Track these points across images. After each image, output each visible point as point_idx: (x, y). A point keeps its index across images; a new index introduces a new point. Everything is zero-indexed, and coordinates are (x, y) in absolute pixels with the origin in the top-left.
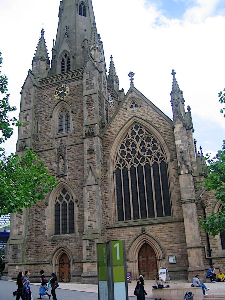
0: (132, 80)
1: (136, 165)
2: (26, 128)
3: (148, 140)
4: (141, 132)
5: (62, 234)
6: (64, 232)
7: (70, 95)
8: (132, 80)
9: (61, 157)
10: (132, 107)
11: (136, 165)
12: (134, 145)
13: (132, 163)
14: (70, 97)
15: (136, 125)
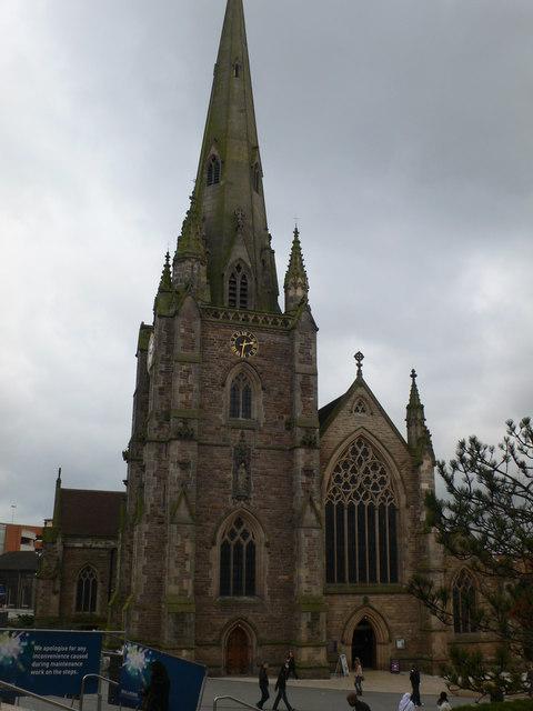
0: (359, 365)
1: (356, 503)
2: (187, 397)
3: (375, 467)
4: (365, 453)
5: (235, 594)
6: (238, 592)
7: (260, 355)
8: (359, 365)
10: (357, 410)
11: (356, 503)
12: (354, 471)
13: (350, 498)
14: (259, 360)
15: (361, 440)
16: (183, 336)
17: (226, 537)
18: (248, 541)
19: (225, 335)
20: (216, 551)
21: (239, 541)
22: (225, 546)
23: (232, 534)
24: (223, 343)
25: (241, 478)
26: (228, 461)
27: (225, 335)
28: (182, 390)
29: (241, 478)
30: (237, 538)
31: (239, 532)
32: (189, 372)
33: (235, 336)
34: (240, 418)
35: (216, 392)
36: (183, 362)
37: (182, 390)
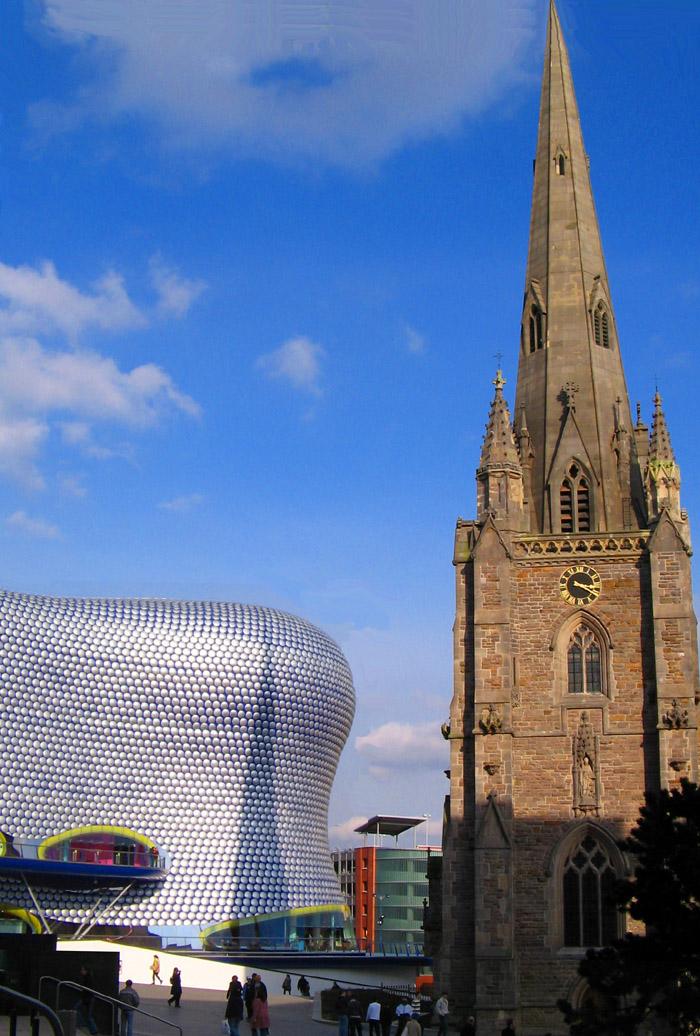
9: (587, 760)
14: (605, 606)
16: (486, 588)
17: (572, 864)
18: (603, 869)
19: (552, 576)
20: (556, 884)
21: (590, 869)
22: (570, 878)
23: (580, 859)
24: (547, 589)
25: (586, 783)
26: (568, 757)
27: (552, 576)
28: (486, 664)
29: (586, 783)
30: (586, 866)
31: (590, 855)
32: (494, 638)
33: (567, 574)
34: (585, 692)
35: (542, 660)
36: (486, 625)
37: (486, 664)
